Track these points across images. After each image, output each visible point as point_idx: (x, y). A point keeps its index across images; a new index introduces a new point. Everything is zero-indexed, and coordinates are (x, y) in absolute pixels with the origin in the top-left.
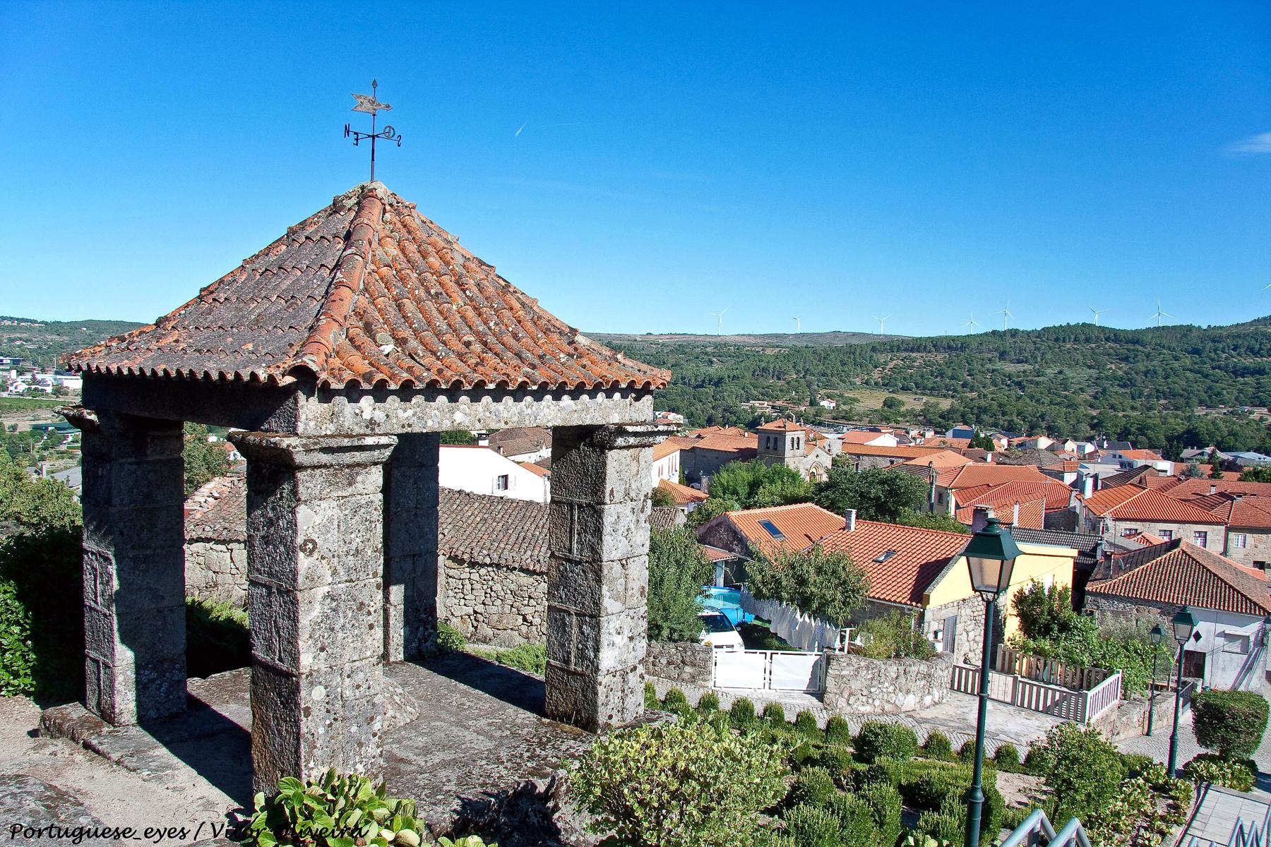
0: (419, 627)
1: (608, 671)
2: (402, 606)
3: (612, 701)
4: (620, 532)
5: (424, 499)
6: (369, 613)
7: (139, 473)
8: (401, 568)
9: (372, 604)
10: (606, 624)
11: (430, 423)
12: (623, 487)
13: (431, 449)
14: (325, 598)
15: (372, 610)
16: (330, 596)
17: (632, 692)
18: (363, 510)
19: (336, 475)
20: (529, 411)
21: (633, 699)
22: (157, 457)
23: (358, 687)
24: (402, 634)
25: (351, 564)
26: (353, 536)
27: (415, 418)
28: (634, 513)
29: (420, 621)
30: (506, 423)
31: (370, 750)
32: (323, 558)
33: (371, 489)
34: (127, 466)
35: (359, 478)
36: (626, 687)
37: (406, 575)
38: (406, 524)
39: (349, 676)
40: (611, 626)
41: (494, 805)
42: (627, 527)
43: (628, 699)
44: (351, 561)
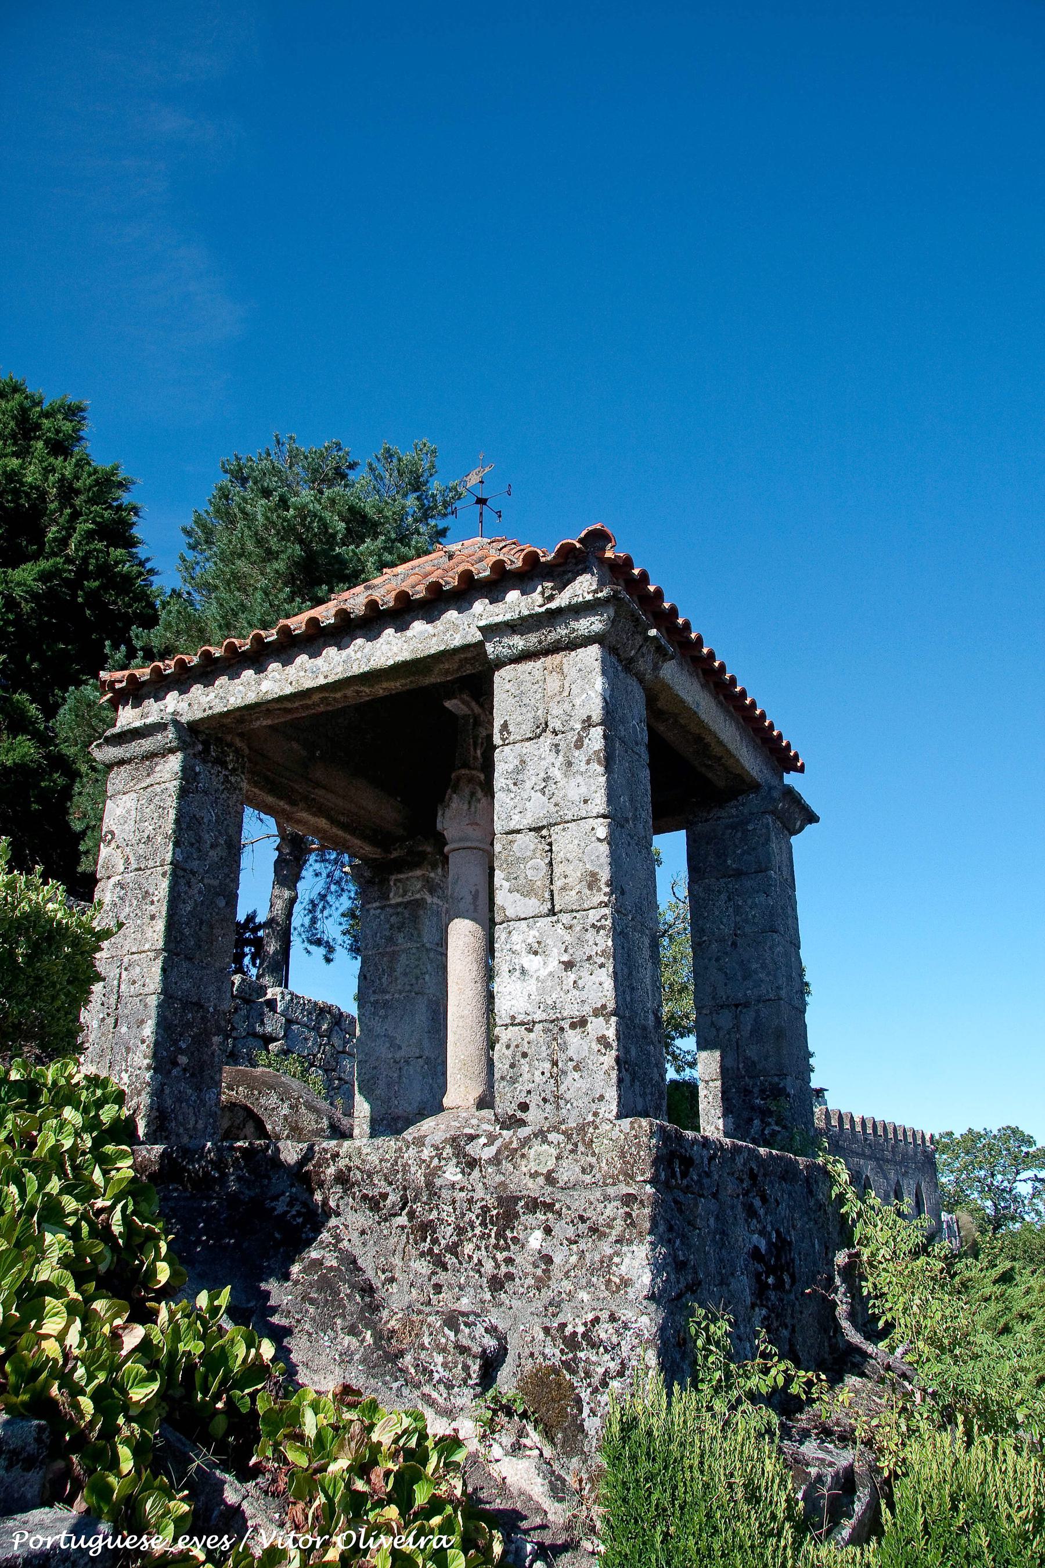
0: (752, 1120)
1: (513, 1018)
2: (719, 1083)
3: (526, 1076)
4: (528, 785)
5: (746, 921)
6: (152, 903)
7: (382, 918)
8: (712, 1023)
9: (156, 893)
10: (503, 936)
11: (232, 700)
12: (530, 715)
13: (754, 849)
14: (115, 886)
15: (155, 899)
16: (121, 885)
17: (576, 1068)
18: (157, 798)
19: (137, 769)
20: (359, 655)
21: (583, 1084)
22: (400, 900)
23: (134, 982)
24: (721, 1127)
25: (141, 852)
26: (146, 824)
27: (217, 700)
28: (558, 752)
29: (753, 1108)
30: (326, 677)
31: (136, 1059)
32: (118, 847)
33: (167, 776)
34: (372, 912)
35: (158, 769)
36: (561, 1057)
37: (721, 1034)
38: (717, 960)
39: (126, 969)
40: (515, 937)
41: (209, 1151)
42: (542, 775)
43: (567, 1081)
44: (141, 849)
